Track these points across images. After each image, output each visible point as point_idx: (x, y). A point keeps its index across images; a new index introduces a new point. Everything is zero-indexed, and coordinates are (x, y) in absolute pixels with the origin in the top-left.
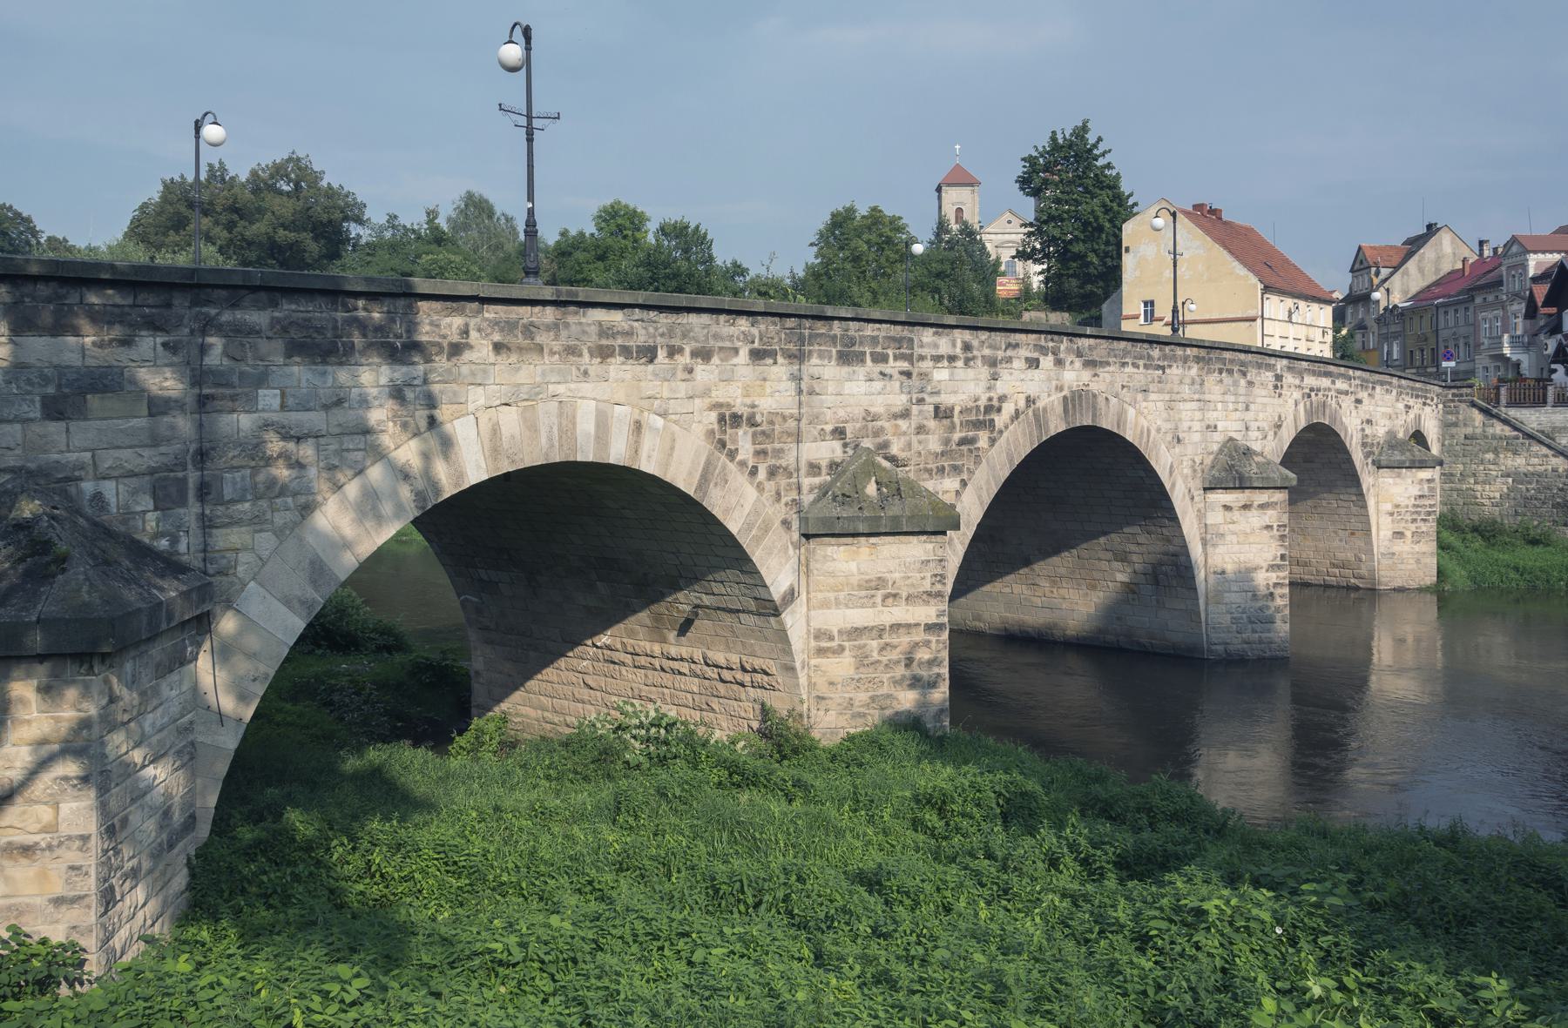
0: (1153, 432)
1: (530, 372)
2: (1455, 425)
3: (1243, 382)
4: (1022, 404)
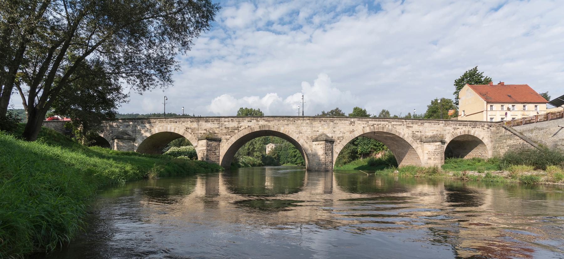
0: (290, 131)
1: (162, 124)
2: (498, 133)
3: (332, 123)
4: (247, 127)
